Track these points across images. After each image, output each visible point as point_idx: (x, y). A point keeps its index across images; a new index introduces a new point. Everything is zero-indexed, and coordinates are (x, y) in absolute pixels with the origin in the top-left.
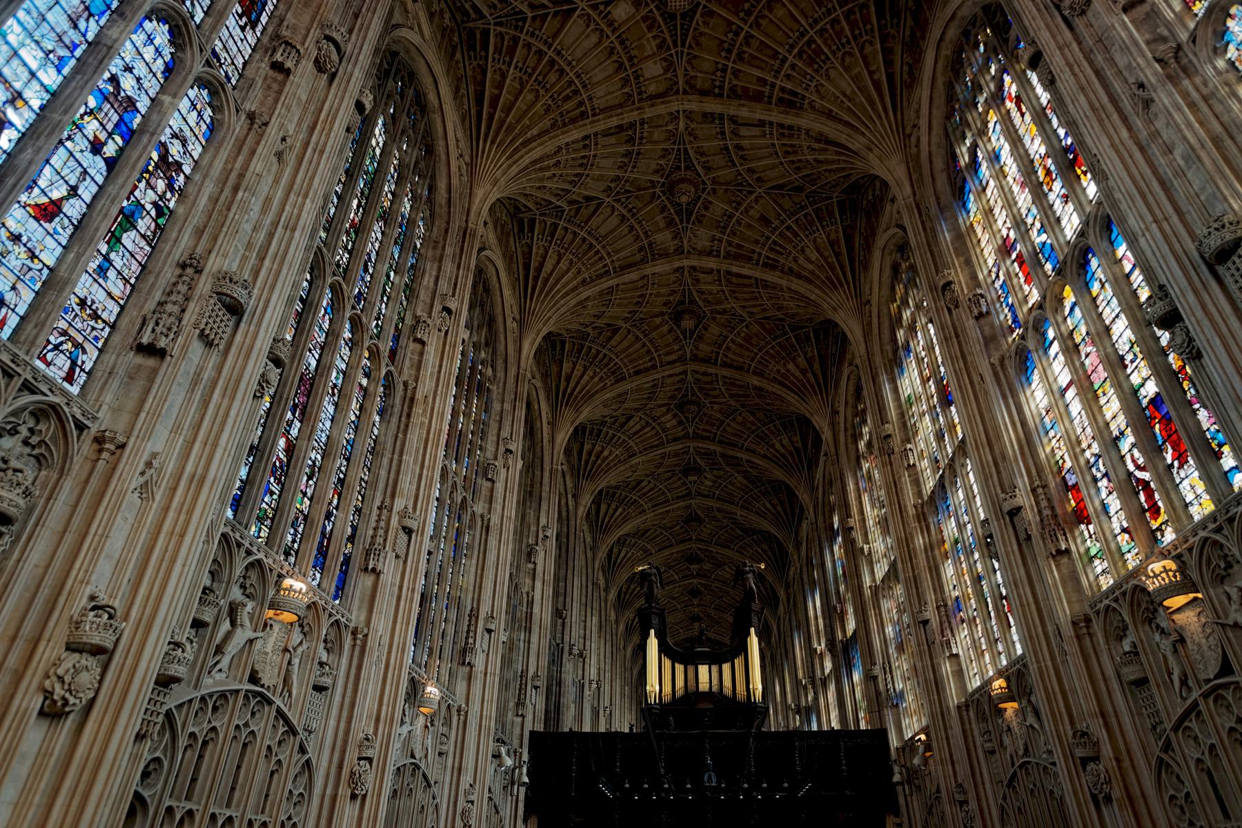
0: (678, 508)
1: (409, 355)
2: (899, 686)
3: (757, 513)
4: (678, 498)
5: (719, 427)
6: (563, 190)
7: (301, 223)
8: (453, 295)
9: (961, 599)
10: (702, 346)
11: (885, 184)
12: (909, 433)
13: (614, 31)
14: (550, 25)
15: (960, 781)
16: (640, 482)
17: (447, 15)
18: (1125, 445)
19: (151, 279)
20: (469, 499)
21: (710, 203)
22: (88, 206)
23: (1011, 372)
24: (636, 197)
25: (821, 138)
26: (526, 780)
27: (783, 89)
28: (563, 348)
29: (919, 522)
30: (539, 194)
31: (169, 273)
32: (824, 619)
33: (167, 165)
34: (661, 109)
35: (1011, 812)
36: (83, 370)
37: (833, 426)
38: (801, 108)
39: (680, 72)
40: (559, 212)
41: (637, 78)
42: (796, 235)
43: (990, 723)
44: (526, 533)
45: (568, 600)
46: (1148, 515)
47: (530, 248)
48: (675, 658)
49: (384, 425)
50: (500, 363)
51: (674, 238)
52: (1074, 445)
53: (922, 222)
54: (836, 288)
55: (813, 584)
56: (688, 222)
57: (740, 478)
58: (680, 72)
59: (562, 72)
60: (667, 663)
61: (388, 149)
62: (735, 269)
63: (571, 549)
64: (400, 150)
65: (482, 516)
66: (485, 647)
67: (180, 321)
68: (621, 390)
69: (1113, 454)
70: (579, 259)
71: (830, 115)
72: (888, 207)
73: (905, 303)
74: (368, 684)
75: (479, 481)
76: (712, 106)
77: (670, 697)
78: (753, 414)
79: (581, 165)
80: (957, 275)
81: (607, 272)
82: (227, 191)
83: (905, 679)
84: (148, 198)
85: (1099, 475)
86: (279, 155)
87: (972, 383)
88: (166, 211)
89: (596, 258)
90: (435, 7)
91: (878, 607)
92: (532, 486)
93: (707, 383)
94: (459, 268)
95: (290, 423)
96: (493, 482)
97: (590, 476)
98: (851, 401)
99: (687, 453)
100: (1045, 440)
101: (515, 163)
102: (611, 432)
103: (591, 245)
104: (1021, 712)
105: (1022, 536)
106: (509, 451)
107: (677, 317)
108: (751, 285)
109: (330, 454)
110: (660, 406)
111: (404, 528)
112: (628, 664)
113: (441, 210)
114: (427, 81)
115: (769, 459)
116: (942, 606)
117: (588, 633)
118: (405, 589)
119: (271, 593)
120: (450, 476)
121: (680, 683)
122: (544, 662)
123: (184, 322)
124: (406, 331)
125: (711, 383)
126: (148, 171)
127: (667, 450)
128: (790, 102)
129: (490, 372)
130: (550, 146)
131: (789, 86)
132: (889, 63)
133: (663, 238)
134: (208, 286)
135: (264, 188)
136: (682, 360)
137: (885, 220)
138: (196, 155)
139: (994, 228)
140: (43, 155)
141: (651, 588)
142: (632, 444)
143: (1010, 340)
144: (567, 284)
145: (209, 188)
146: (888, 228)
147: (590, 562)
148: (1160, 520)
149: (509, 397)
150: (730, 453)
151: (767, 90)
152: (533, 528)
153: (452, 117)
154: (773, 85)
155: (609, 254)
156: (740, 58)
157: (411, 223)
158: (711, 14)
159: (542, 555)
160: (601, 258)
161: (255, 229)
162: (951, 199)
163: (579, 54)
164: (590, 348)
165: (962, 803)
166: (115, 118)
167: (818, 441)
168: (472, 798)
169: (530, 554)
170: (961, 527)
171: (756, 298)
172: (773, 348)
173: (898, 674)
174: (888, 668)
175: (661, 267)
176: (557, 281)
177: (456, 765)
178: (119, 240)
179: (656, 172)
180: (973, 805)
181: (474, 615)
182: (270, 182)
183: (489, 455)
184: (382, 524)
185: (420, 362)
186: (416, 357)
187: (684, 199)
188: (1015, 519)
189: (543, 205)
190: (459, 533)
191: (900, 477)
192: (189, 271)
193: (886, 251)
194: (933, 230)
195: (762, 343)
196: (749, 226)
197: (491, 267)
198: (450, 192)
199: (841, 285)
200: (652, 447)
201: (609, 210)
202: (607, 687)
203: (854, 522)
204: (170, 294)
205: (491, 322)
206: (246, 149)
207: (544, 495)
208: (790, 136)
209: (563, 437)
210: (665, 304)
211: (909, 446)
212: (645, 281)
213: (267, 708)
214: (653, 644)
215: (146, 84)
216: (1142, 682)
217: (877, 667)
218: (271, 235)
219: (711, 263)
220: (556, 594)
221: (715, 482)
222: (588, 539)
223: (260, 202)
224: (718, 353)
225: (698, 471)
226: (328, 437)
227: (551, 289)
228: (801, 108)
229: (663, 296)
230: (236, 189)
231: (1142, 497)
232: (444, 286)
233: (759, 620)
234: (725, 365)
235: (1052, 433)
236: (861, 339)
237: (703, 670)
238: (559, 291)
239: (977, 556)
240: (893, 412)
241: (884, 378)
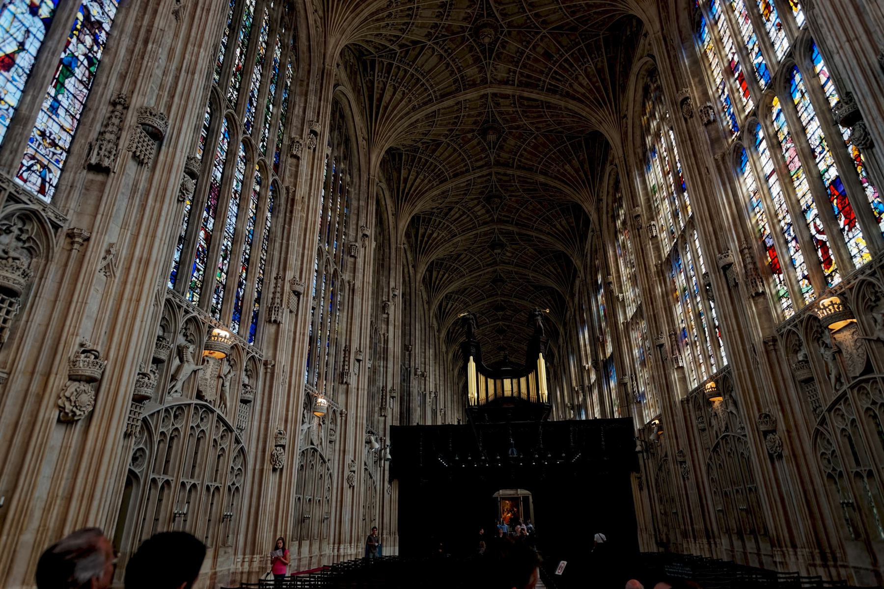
0: (488, 273)
1: (288, 167)
2: (642, 389)
3: (543, 274)
4: (487, 265)
5: (516, 213)
6: (395, 36)
7: (199, 67)
8: (318, 121)
9: (687, 330)
10: (502, 154)
11: (640, 22)
12: (653, 212)
15: (681, 449)
16: (460, 255)
18: (810, 216)
20: (339, 270)
21: (507, 42)
22: (36, 58)
23: (730, 164)
24: (451, 40)
26: (389, 457)
28: (400, 159)
29: (659, 277)
30: (377, 41)
31: (104, 110)
32: (591, 346)
33: (92, 25)
35: (714, 468)
36: (51, 185)
37: (599, 210)
40: (392, 54)
42: (571, 66)
43: (703, 411)
44: (380, 293)
46: (823, 265)
47: (372, 82)
48: (487, 376)
49: (274, 219)
50: (355, 172)
51: (480, 72)
52: (773, 217)
53: (668, 52)
54: (602, 107)
55: (583, 322)
56: (490, 59)
57: (531, 250)
60: (482, 378)
61: (259, 8)
62: (526, 94)
63: (413, 304)
64: (269, 7)
65: (349, 282)
66: (357, 372)
67: (117, 145)
68: (444, 188)
69: (801, 222)
70: (410, 91)
72: (642, 41)
73: (653, 116)
74: (277, 398)
75: (345, 257)
78: (540, 203)
79: (408, 15)
80: (693, 92)
81: (431, 100)
82: (140, 44)
83: (645, 384)
84: (80, 51)
85: (790, 238)
86: (176, 13)
87: (700, 174)
88: (95, 61)
89: (422, 89)
92: (383, 260)
93: (505, 181)
94: (320, 100)
95: (206, 220)
96: (355, 258)
97: (425, 252)
98: (611, 191)
99: (493, 233)
100: (752, 215)
101: (357, 15)
102: (438, 220)
103: (418, 79)
104: (725, 404)
105: (732, 284)
106: (365, 235)
107: (484, 133)
108: (538, 107)
109: (237, 241)
110: (472, 200)
111: (294, 292)
112: (456, 380)
113: (304, 56)
115: (552, 235)
116: (673, 334)
117: (427, 360)
118: (298, 334)
119: (205, 339)
120: (324, 254)
122: (398, 380)
123: (120, 147)
124: (284, 149)
125: (509, 181)
126: (77, 29)
127: (479, 231)
129: (348, 178)
133: (472, 72)
134: (135, 119)
135: (168, 40)
136: (488, 165)
137: (639, 51)
138: (112, 14)
139: (723, 53)
141: (469, 329)
142: (453, 227)
143: (730, 140)
144: (402, 110)
145: (125, 42)
146: (641, 57)
147: (426, 312)
148: (831, 269)
149: (363, 197)
150: (525, 232)
152: (386, 290)
155: (431, 86)
157: (282, 66)
159: (392, 308)
160: (426, 89)
161: (164, 73)
162: (691, 32)
164: (420, 158)
165: (681, 463)
167: (587, 221)
168: (355, 469)
169: (384, 308)
170: (688, 279)
171: (541, 116)
172: (554, 153)
173: (641, 381)
174: (634, 377)
175: (471, 95)
176: (394, 109)
177: (342, 448)
178: (63, 85)
179: (465, 19)
180: (689, 463)
181: (347, 350)
182: (171, 35)
183: (351, 238)
184: (279, 289)
185: (297, 172)
186: (294, 169)
187: (487, 40)
188: (728, 272)
189: (380, 48)
190: (333, 294)
191: (646, 246)
192: (119, 107)
193: (639, 77)
194: (675, 56)
195: (547, 150)
196: (536, 60)
197: (344, 99)
198: (309, 41)
199: (606, 104)
200: (468, 230)
201: (430, 51)
202: (442, 396)
203: (612, 278)
204: (107, 125)
205: (347, 141)
207: (392, 266)
209: (403, 224)
210: (475, 123)
211: (653, 223)
212: (459, 106)
213: (210, 415)
214: (472, 366)
216: (809, 381)
217: (627, 377)
218: (177, 78)
219: (508, 90)
220: (404, 334)
221: (513, 253)
222: (425, 296)
224: (514, 159)
225: (502, 246)
226: (235, 229)
227: (390, 114)
229: (473, 116)
230: (146, 42)
231: (820, 254)
232: (310, 115)
233: (546, 348)
234: (519, 168)
235: (757, 210)
236: (620, 145)
237: (507, 382)
238: (396, 116)
239: (699, 299)
240: (642, 198)
241: (636, 173)
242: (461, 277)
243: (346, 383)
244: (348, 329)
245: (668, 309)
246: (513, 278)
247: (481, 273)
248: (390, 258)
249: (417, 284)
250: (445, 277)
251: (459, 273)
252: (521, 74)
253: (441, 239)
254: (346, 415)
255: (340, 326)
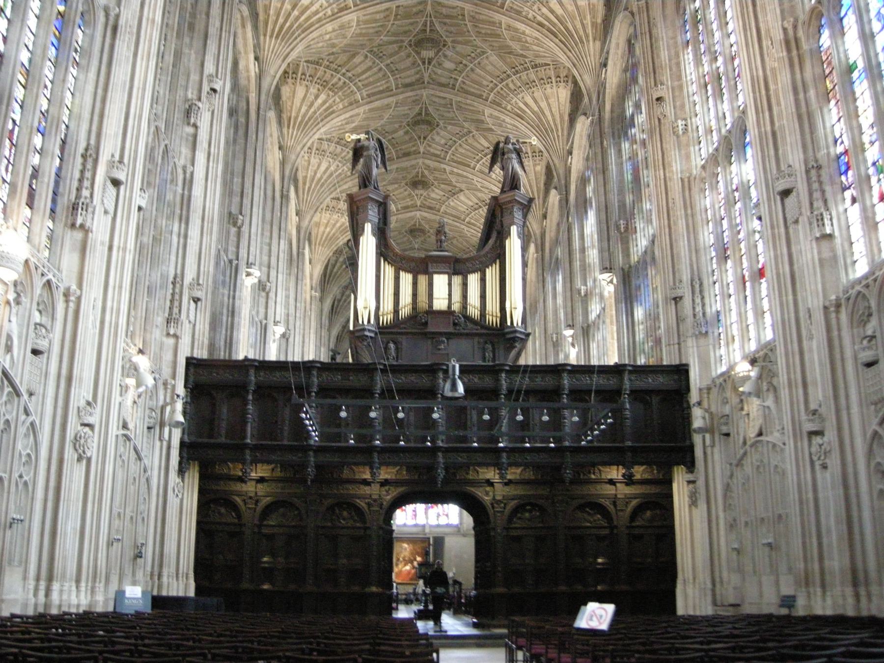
4: (406, 86)
29: (789, 50)
45: (247, 202)
57: (494, 58)
60: (388, 271)
77: (390, 317)
91: (689, 205)
92: (193, 15)
116: (813, 168)
121: (406, 298)
141: (368, 167)
152: (194, 77)
168: (93, 420)
181: (91, 155)
207: (213, 31)
214: (368, 243)
220: (227, 185)
237: (440, 281)
242: (351, 104)
243: (82, 226)
244: (97, 111)
245: (805, 117)
246: (453, 119)
247: (391, 99)
248: (208, 15)
249: (263, 97)
250: (320, 101)
251: (348, 96)
253: (317, 12)
254: (79, 299)
255: (77, 101)
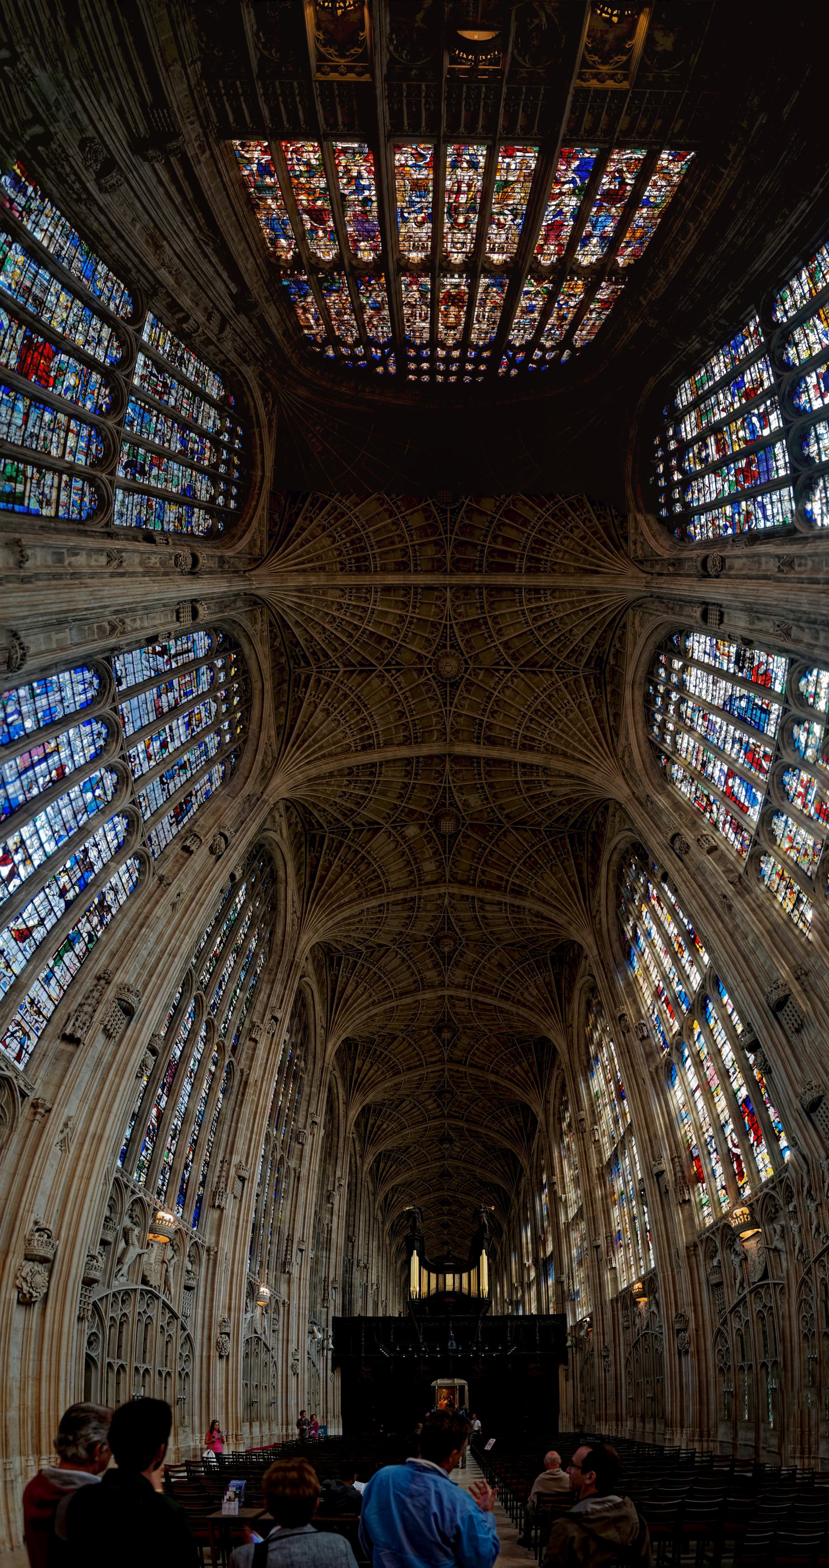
7: (181, 951)
13: (406, 842)
14: (364, 835)
17: (300, 825)
19: (77, 987)
22: (48, 932)
25: (538, 915)
27: (514, 884)
31: (89, 983)
34: (434, 891)
38: (526, 895)
39: (447, 870)
40: (359, 953)
41: (419, 870)
42: (522, 977)
51: (439, 975)
58: (447, 870)
59: (369, 864)
62: (480, 999)
67: (92, 1018)
71: (543, 901)
76: (468, 891)
82: (136, 928)
84: (85, 928)
86: (174, 905)
90: (293, 820)
113: (277, 948)
114: (279, 863)
126: (89, 911)
128: (518, 892)
130: (356, 910)
131: (517, 882)
132: (580, 872)
133: (431, 975)
135: (160, 927)
138: (121, 902)
140: (30, 897)
145: (125, 924)
151: (503, 883)
153: (292, 886)
154: (507, 881)
156: (486, 863)
157: (255, 955)
158: (468, 836)
161: (149, 955)
163: (382, 854)
166: (79, 875)
178: (61, 958)
179: (428, 930)
182: (165, 921)
187: (446, 949)
192: (102, 982)
196: (491, 970)
198: (284, 936)
204: (87, 998)
206: (153, 900)
208: (519, 912)
215: (103, 855)
218: (159, 959)
219: (464, 994)
223: (155, 936)
228: (526, 895)
230: (141, 926)
252: (477, 981)
